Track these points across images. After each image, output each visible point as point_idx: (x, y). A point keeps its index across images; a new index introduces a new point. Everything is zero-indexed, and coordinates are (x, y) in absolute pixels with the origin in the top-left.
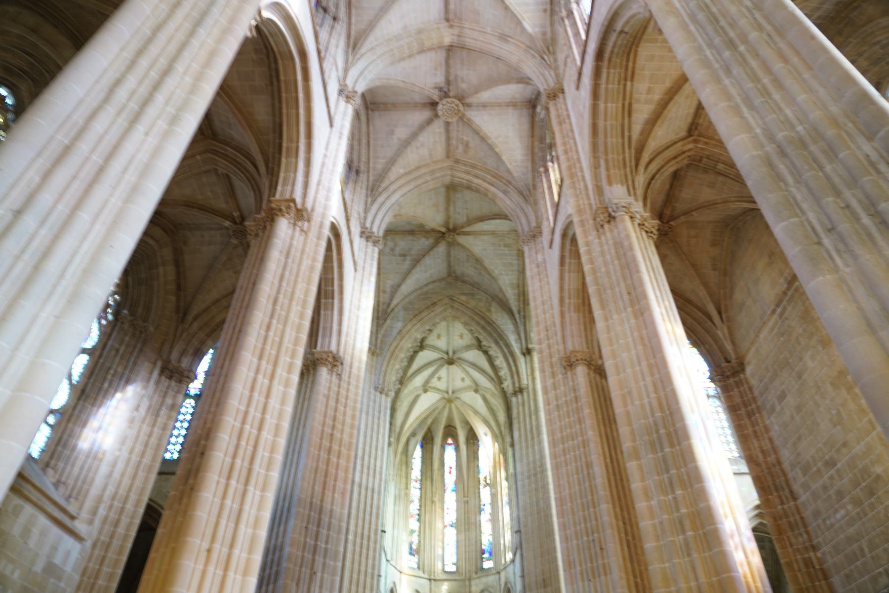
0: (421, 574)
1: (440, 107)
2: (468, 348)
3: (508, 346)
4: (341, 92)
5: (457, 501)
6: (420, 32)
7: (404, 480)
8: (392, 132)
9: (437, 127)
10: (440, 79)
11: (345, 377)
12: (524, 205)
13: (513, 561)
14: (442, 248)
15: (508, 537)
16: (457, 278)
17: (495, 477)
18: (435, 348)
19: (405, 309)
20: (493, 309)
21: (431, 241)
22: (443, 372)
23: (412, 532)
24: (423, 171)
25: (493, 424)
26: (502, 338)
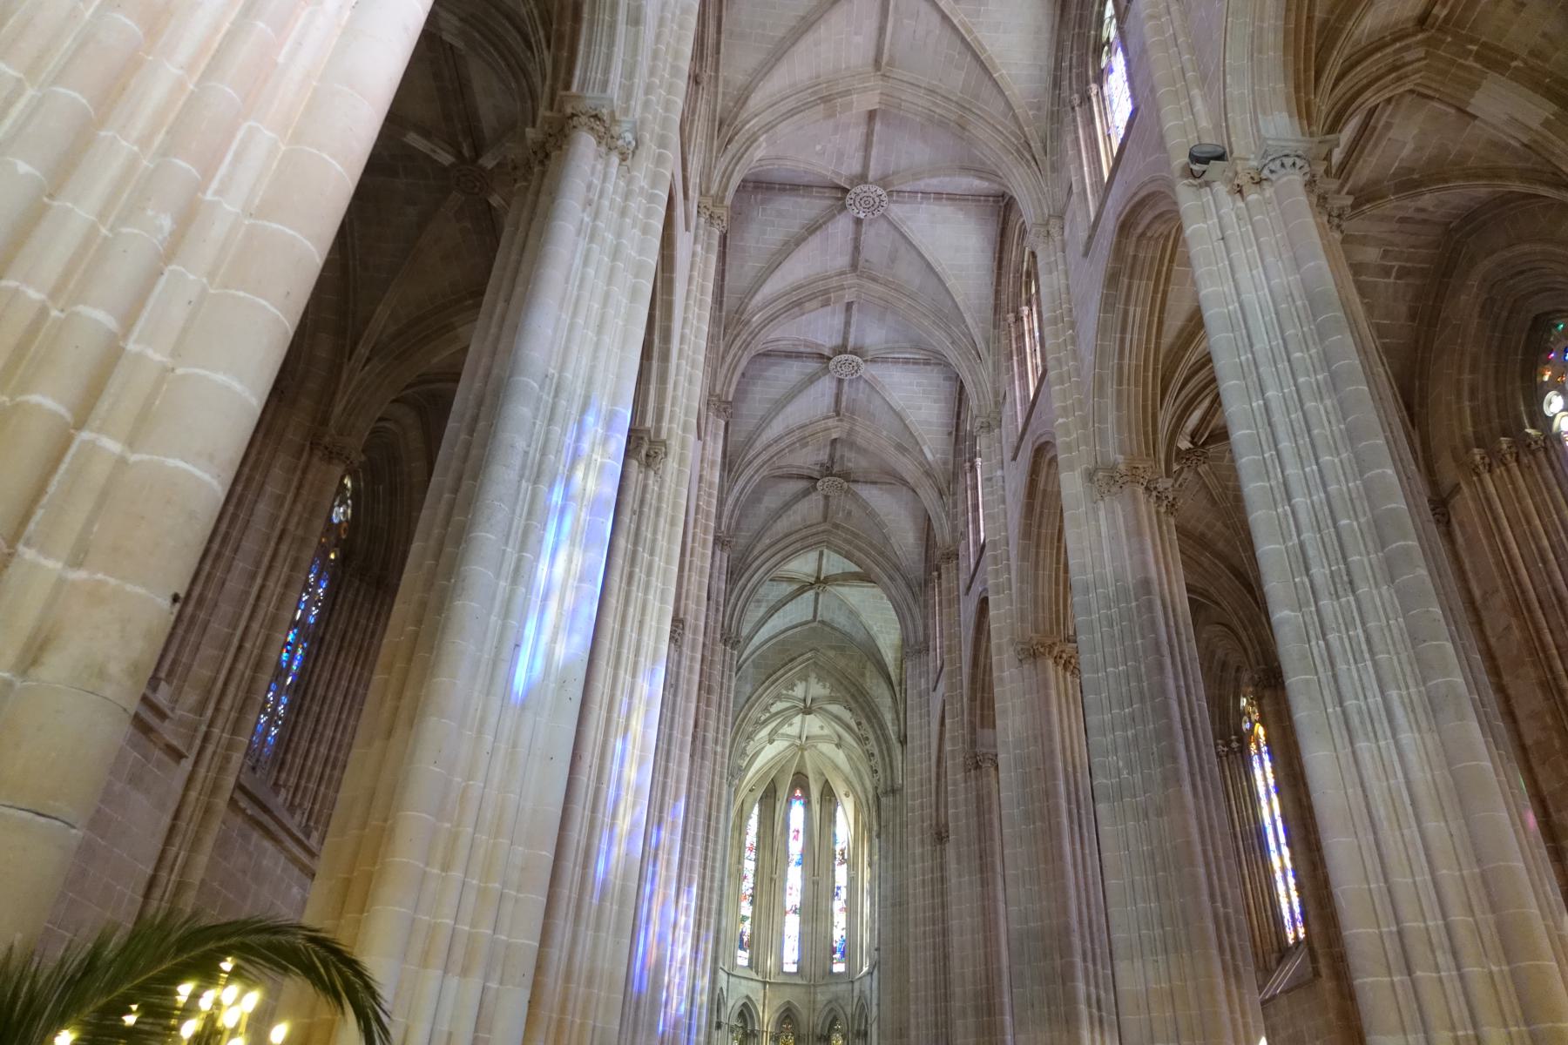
0: (754, 975)
1: (819, 483)
2: (832, 700)
3: (882, 727)
4: (717, 540)
5: (804, 879)
9: (816, 499)
10: (824, 456)
13: (870, 973)
14: (810, 595)
15: (866, 938)
16: (823, 622)
17: (856, 855)
18: (788, 698)
19: (756, 665)
21: (795, 586)
22: (797, 720)
23: (744, 919)
24: (793, 538)
25: (858, 788)
26: (875, 715)
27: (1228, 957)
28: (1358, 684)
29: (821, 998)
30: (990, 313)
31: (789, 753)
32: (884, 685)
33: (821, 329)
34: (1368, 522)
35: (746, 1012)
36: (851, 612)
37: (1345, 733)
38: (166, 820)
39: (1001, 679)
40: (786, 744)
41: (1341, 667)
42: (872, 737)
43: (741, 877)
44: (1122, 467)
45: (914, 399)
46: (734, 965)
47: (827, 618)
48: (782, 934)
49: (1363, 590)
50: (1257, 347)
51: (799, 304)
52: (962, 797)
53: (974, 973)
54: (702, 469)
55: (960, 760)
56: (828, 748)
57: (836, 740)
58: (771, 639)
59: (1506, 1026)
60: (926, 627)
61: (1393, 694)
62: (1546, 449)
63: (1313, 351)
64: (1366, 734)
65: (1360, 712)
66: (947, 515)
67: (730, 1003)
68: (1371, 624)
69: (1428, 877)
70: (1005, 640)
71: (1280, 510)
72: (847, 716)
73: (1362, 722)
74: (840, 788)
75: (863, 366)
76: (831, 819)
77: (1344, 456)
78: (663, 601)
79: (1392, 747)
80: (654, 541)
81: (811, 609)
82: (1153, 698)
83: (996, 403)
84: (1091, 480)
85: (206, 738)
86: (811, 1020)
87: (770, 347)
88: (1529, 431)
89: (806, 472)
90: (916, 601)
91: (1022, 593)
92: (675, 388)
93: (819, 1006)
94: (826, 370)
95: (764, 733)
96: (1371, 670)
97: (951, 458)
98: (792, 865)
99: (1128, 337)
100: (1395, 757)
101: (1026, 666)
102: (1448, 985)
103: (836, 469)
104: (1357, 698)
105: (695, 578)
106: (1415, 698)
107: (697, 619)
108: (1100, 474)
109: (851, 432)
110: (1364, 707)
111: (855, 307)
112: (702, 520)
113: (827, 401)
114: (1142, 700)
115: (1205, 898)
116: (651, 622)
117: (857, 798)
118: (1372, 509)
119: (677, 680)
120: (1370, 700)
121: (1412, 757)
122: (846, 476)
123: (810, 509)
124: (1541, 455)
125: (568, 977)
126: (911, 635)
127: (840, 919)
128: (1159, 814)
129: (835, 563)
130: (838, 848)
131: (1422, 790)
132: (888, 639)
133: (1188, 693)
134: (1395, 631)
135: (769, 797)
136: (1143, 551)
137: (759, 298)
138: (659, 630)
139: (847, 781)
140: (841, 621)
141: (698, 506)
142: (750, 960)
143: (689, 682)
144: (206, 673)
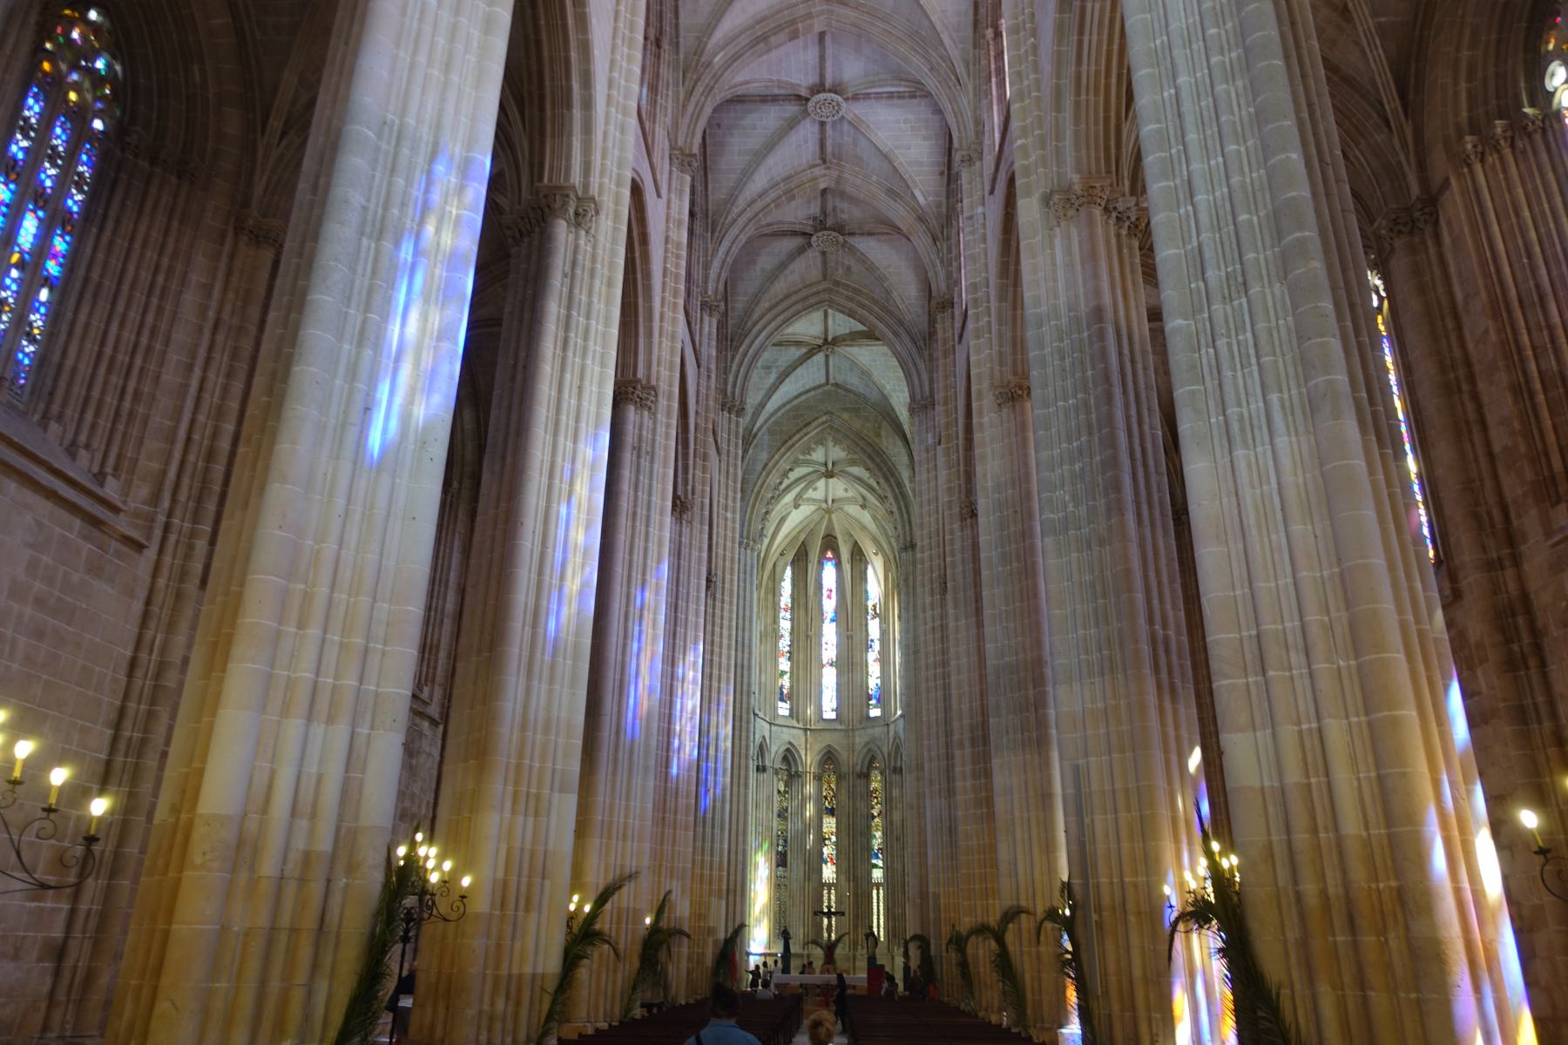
0: (795, 723)
1: (814, 239)
2: (853, 463)
3: (900, 485)
4: (704, 305)
5: (838, 634)
6: (788, 178)
7: (770, 612)
8: (754, 262)
9: (812, 255)
10: (815, 209)
11: (718, 596)
12: (916, 356)
14: (819, 358)
15: (897, 684)
18: (808, 463)
19: (771, 432)
20: (883, 433)
21: (804, 350)
22: (821, 483)
23: (783, 673)
24: (794, 298)
25: (885, 546)
26: (893, 475)
27: (1164, 676)
28: (1242, 391)
29: (860, 739)
30: (969, 32)
31: (816, 517)
32: (900, 443)
33: (793, 65)
34: (1267, 215)
35: (789, 756)
36: (863, 372)
37: (1225, 443)
38: (138, 606)
39: (981, 425)
40: (813, 508)
41: (1227, 373)
42: (890, 495)
43: (777, 636)
44: (1077, 188)
45: (898, 136)
46: (775, 715)
47: (840, 380)
48: (820, 685)
49: (1255, 289)
50: (1173, 26)
51: (764, 38)
52: (958, 545)
53: (971, 708)
54: (668, 229)
55: (956, 510)
56: (853, 510)
57: (860, 500)
58: (784, 405)
59: (1347, 717)
60: (931, 381)
61: (1274, 397)
62: (1544, 130)
63: (1229, 25)
64: (1245, 442)
65: (1241, 420)
66: (942, 261)
67: (774, 749)
68: (1261, 325)
69: (1290, 580)
70: (986, 384)
71: (1182, 211)
72: (865, 475)
73: (1242, 430)
74: (869, 549)
75: (844, 105)
76: (864, 578)
77: (1250, 143)
78: (603, 365)
79: (1269, 453)
80: (590, 304)
81: (823, 372)
82: (1100, 430)
83: (977, 133)
84: (1048, 205)
85: (167, 528)
86: (850, 759)
87: (740, 91)
88: (1528, 110)
89: (797, 228)
90: (921, 355)
91: (1000, 336)
92: (605, 140)
93: (858, 748)
94: (806, 113)
95: (789, 498)
96: (1256, 374)
97: (944, 200)
98: (827, 622)
99: (1086, 39)
100: (1271, 463)
101: (1005, 410)
102: (1298, 682)
103: (829, 222)
104: (1239, 405)
105: (666, 344)
106: (1296, 401)
107: (671, 385)
108: (1056, 197)
109: (839, 179)
110: (1246, 414)
111: (828, 39)
112: (670, 284)
113: (812, 147)
114: (1090, 434)
115: (1142, 621)
116: (591, 389)
117: (885, 555)
118: (1272, 199)
119: (653, 446)
120: (1252, 407)
121: (1286, 462)
122: (840, 229)
123: (806, 268)
124: (1538, 138)
125: (524, 727)
126: (918, 391)
127: (874, 670)
128: (1102, 543)
129: (841, 324)
130: (870, 604)
131: (1291, 494)
132: (900, 400)
133: (1140, 423)
134: (1283, 331)
135: (800, 559)
136: (1096, 276)
137: (718, 35)
138: (600, 394)
139: (875, 540)
140: (854, 381)
141: (665, 269)
142: (791, 710)
143: (666, 448)
144: (156, 466)
